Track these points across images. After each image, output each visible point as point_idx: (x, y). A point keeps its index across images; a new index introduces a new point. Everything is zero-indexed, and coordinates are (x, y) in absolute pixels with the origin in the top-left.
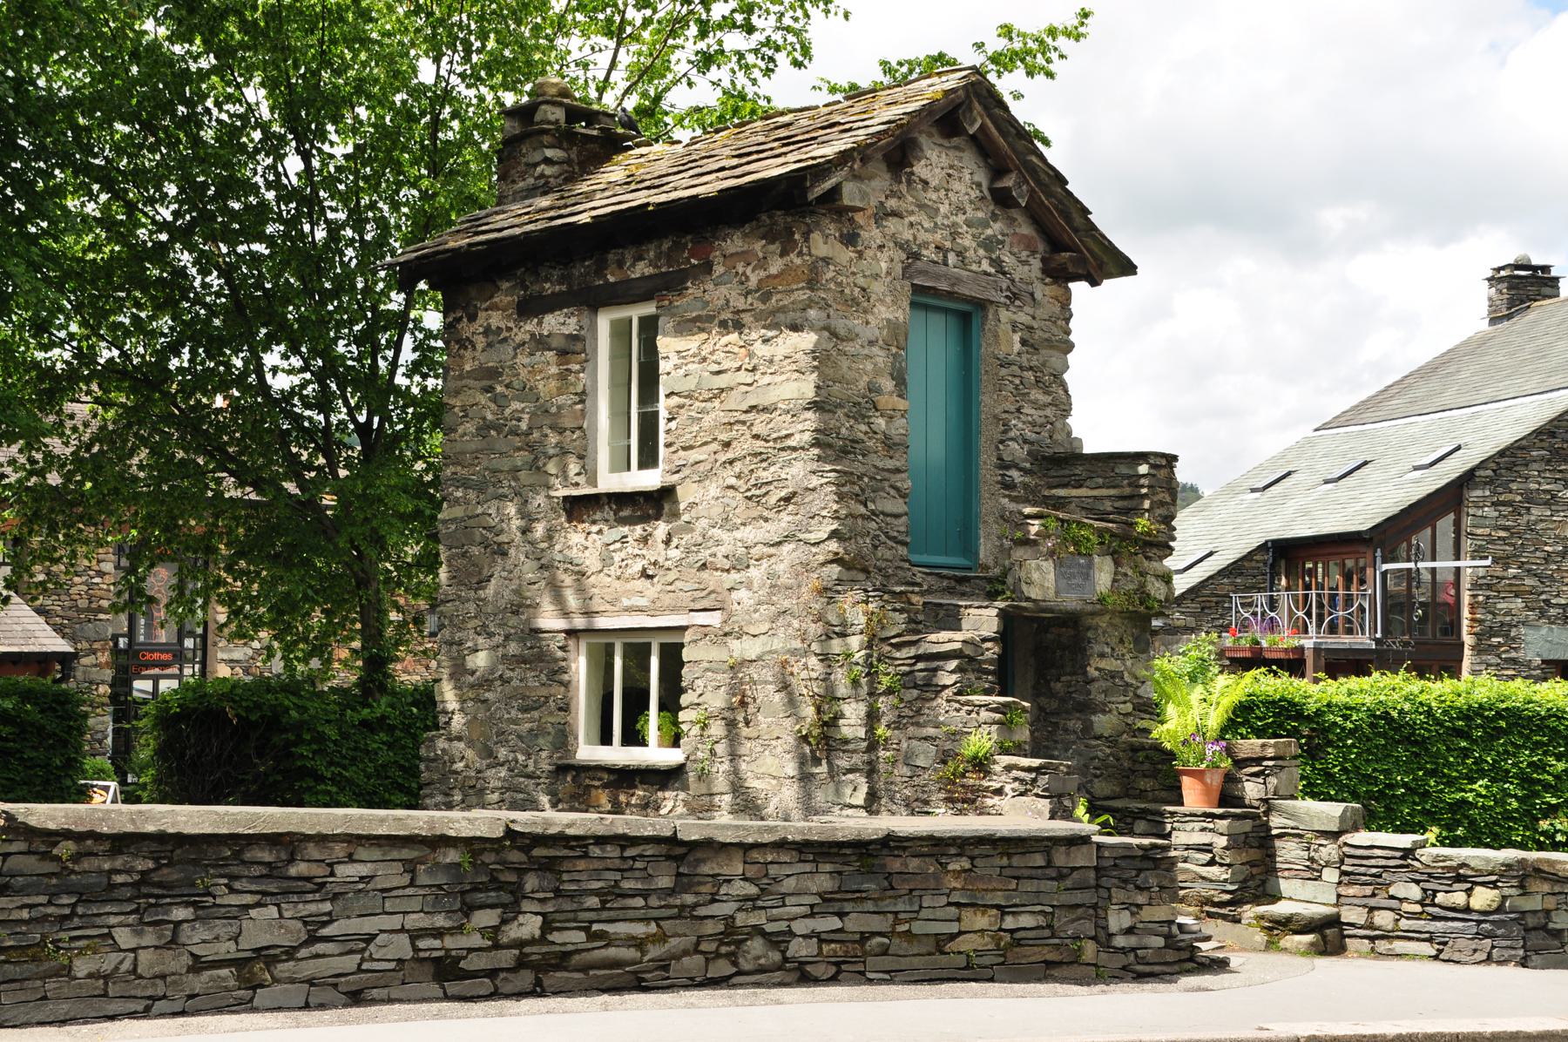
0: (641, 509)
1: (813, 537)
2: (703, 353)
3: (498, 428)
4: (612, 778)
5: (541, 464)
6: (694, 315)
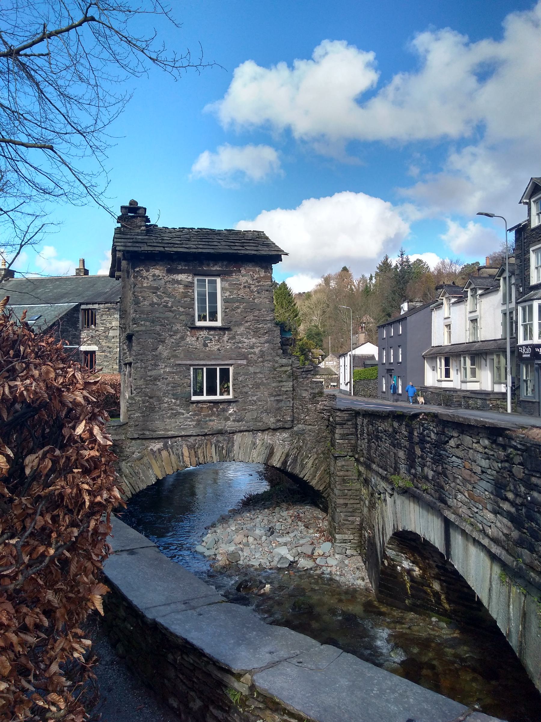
3: (159, 305)
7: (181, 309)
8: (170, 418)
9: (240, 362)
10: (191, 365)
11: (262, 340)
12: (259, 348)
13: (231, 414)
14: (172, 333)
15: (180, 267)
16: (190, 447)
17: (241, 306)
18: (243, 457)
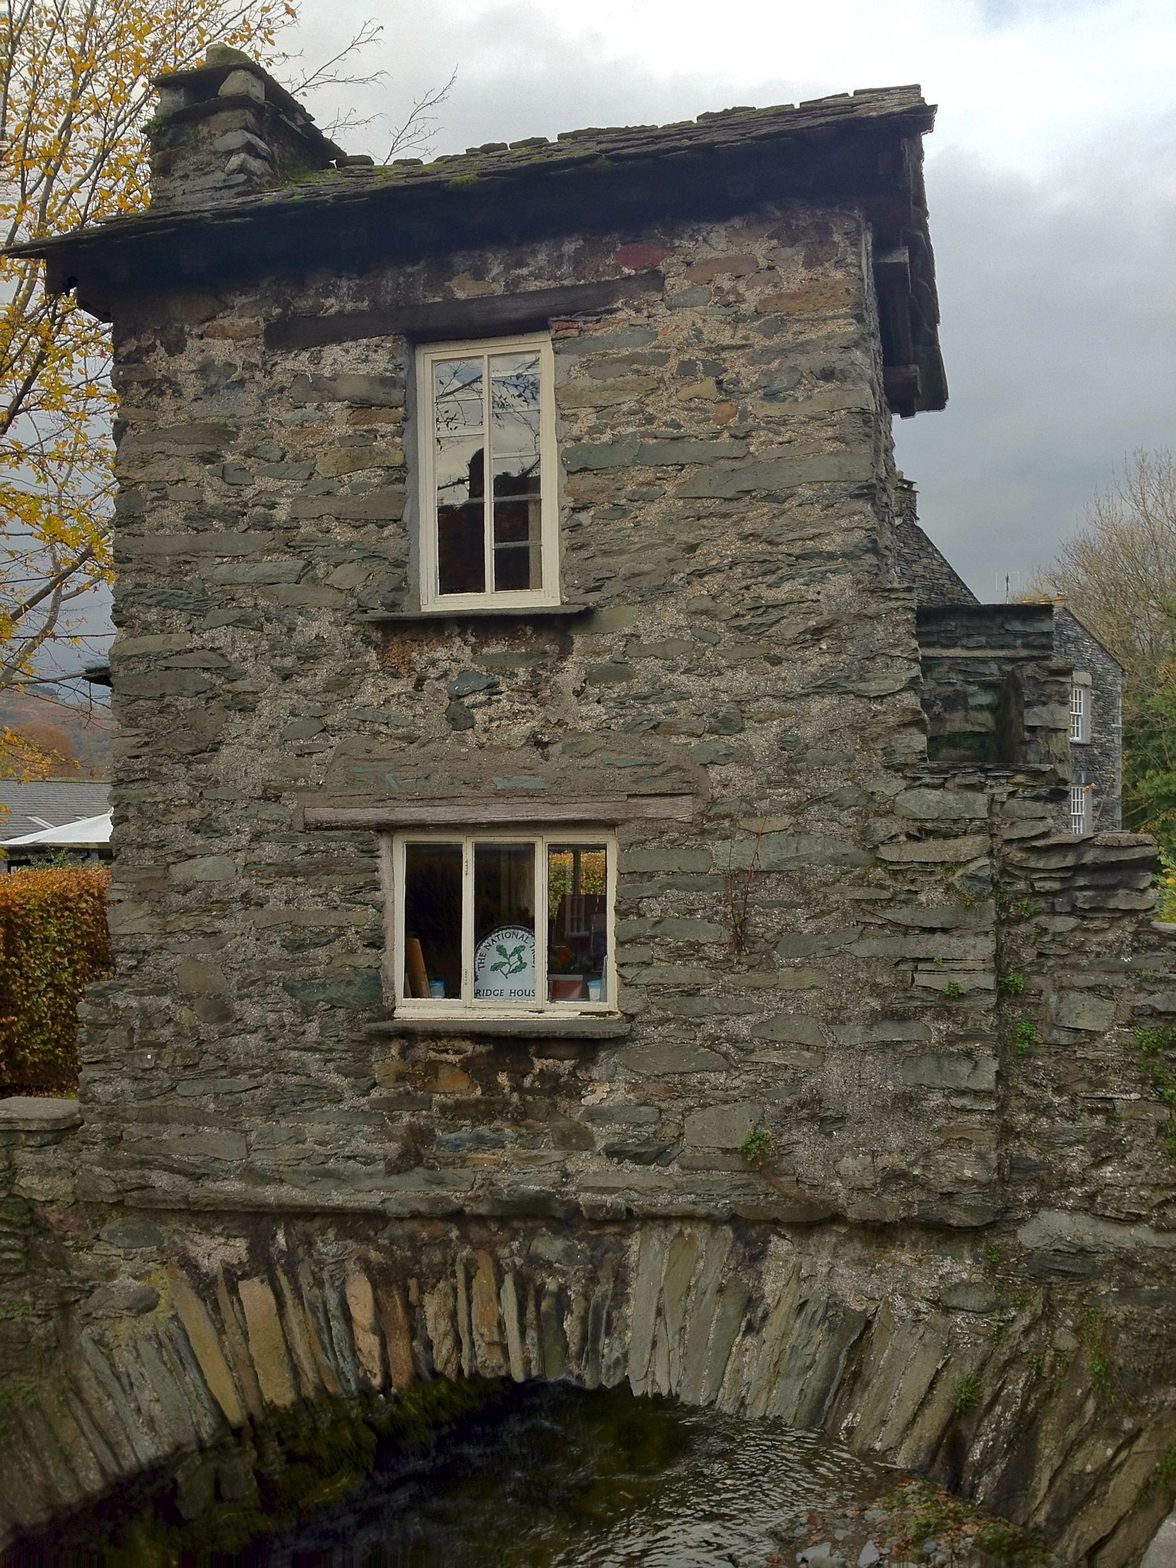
0: (527, 643)
1: (874, 688)
2: (650, 410)
4: (480, 1048)
5: (320, 573)
6: (625, 352)
7: (342, 534)
8: (269, 1110)
9: (656, 808)
10: (387, 829)
11: (791, 676)
12: (775, 727)
13: (594, 1115)
14: (288, 662)
15: (332, 304)
16: (380, 1278)
17: (670, 489)
18: (677, 1369)
